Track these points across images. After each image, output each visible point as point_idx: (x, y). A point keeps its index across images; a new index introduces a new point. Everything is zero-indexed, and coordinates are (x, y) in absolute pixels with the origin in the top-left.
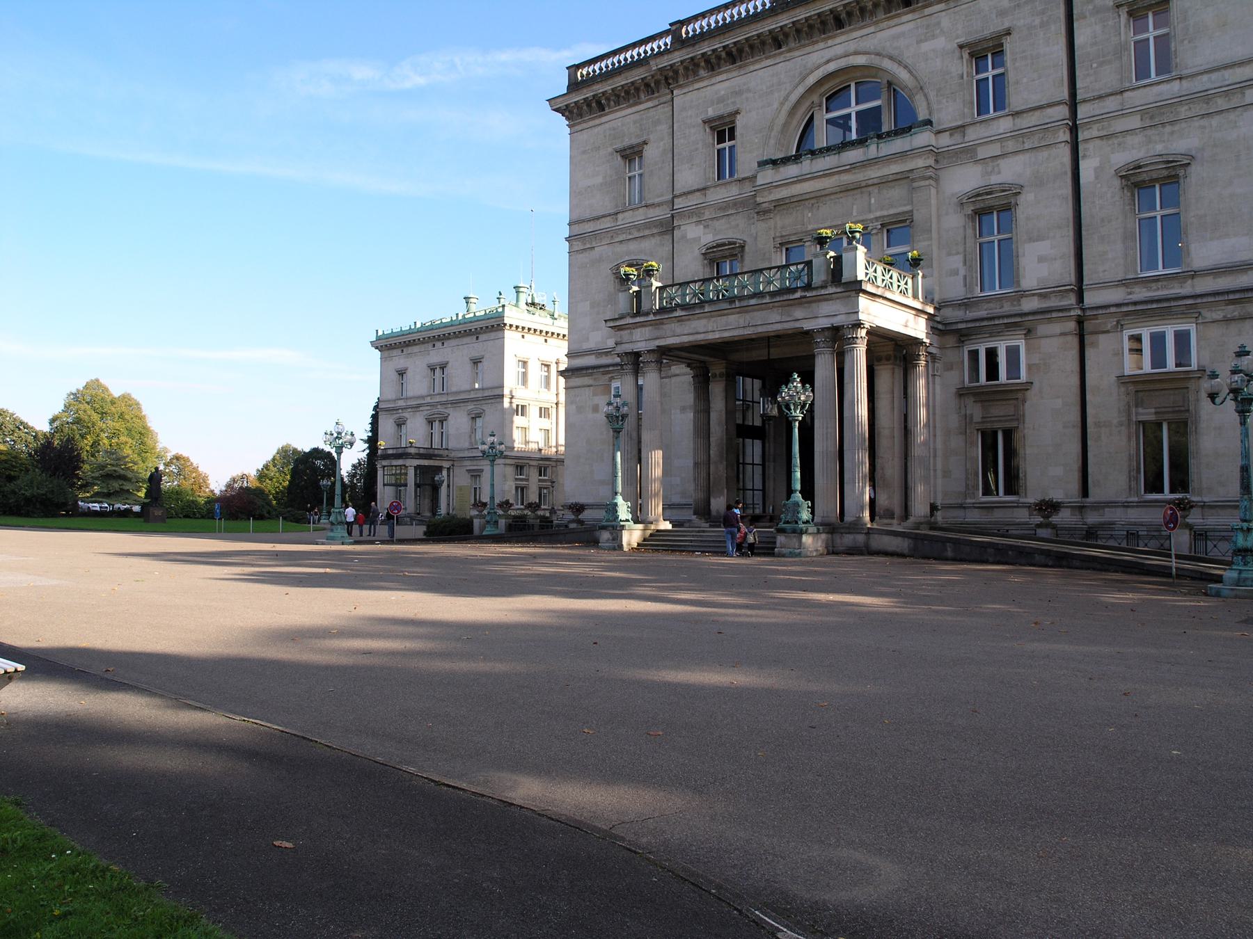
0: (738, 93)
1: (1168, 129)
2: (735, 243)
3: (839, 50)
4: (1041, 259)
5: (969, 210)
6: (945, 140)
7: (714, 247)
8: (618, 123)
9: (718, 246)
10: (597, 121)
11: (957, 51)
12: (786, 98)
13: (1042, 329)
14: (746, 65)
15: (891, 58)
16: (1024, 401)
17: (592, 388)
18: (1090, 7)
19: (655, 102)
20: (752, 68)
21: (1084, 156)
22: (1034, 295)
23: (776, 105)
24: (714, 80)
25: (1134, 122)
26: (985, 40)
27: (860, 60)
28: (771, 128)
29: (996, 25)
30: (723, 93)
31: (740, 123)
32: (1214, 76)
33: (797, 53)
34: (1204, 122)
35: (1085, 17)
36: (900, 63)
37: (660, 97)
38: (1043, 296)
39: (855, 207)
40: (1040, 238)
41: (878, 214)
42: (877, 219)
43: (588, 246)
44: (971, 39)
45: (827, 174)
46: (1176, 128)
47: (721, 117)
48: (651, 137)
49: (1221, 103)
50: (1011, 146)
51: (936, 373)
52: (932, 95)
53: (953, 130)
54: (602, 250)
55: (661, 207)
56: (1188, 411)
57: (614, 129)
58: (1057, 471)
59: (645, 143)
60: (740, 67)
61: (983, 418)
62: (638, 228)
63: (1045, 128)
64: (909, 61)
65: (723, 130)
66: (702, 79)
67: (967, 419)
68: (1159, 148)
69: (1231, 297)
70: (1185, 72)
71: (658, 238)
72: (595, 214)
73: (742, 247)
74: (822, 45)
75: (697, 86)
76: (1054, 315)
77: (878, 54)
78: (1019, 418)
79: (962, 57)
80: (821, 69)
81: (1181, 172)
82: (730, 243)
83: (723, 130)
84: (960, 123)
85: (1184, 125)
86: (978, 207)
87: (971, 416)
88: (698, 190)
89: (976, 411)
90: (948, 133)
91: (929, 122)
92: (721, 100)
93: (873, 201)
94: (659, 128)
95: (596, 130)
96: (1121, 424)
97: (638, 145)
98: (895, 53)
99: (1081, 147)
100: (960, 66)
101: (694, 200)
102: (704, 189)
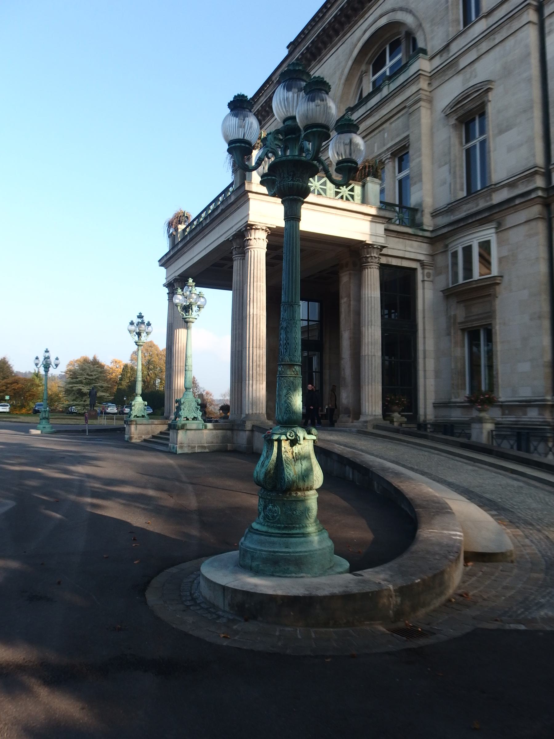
4: (510, 149)
5: (453, 121)
12: (343, 71)
13: (513, 219)
16: (495, 296)
21: (550, 32)
22: (503, 187)
27: (383, 21)
38: (511, 185)
39: (376, 145)
40: (508, 128)
51: (426, 279)
58: (525, 367)
61: (466, 317)
67: (451, 321)
76: (517, 202)
78: (491, 315)
86: (459, 115)
87: (455, 316)
89: (460, 313)
90: (438, 56)
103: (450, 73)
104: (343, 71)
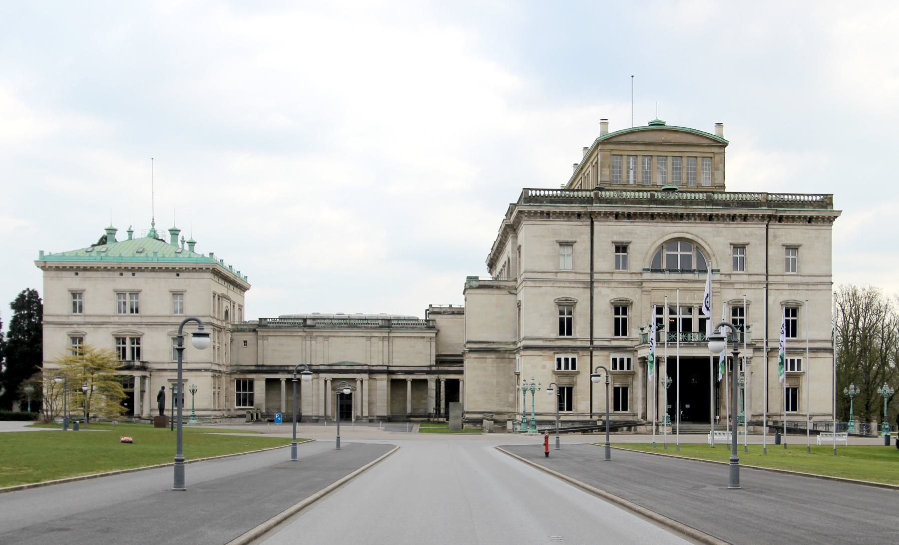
0: (631, 233)
1: (796, 291)
2: (628, 301)
3: (680, 229)
6: (723, 278)
7: (618, 301)
8: (558, 227)
9: (620, 300)
10: (544, 223)
11: (729, 245)
12: (655, 243)
14: (634, 222)
15: (702, 239)
17: (541, 357)
18: (774, 242)
19: (581, 223)
20: (637, 224)
23: (649, 244)
24: (617, 223)
25: (786, 287)
26: (740, 245)
28: (647, 254)
29: (746, 241)
30: (622, 231)
31: (631, 246)
32: (810, 278)
33: (660, 224)
34: (807, 292)
35: (772, 245)
36: (706, 242)
37: (584, 221)
39: (687, 297)
41: (698, 302)
42: (697, 303)
43: (538, 285)
44: (735, 242)
45: (678, 281)
46: (799, 291)
47: (623, 243)
48: (578, 240)
49: (812, 287)
50: (747, 286)
52: (718, 259)
53: (726, 275)
54: (546, 288)
55: (583, 275)
56: (799, 385)
57: (554, 229)
59: (575, 242)
60: (632, 222)
62: (570, 282)
63: (759, 283)
64: (710, 243)
65: (621, 248)
66: (610, 221)
68: (793, 298)
69: (814, 350)
70: (802, 274)
71: (582, 290)
72: (542, 270)
73: (632, 303)
74: (672, 225)
75: (607, 223)
77: (697, 236)
79: (730, 248)
80: (671, 235)
81: (800, 307)
82: (626, 301)
83: (621, 248)
84: (729, 273)
85: (801, 291)
88: (609, 273)
91: (719, 271)
92: (620, 234)
93: (696, 296)
94: (583, 236)
95: (544, 226)
96: (779, 388)
97: (571, 242)
98: (703, 238)
99: (769, 291)
100: (729, 251)
101: (606, 277)
102: (612, 273)
103: (730, 286)
104: (655, 243)
